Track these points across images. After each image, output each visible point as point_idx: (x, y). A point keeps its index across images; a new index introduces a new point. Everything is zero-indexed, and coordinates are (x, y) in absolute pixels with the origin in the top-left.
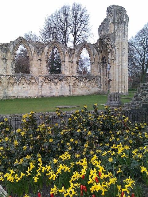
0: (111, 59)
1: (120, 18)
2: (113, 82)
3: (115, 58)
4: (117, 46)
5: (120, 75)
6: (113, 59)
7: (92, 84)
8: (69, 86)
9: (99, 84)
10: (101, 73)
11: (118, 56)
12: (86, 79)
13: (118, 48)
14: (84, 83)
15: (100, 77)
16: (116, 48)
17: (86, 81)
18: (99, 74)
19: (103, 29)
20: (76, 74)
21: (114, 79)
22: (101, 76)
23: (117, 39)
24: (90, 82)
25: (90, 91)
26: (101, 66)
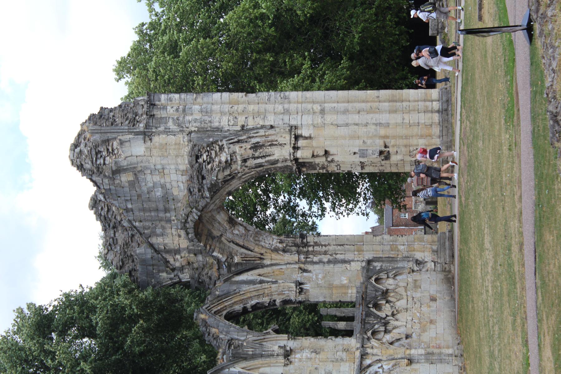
0: (296, 148)
1: (130, 116)
2: (394, 137)
3: (292, 128)
4: (241, 120)
5: (363, 105)
6: (297, 137)
7: (401, 290)
8: (411, 361)
9: (400, 265)
10: (349, 256)
11: (286, 118)
12: (377, 306)
13: (250, 119)
14: (399, 316)
15: (369, 262)
16: (251, 124)
17: (386, 310)
18: (357, 266)
19: (153, 240)
20: (352, 342)
21: (382, 132)
22: (369, 256)
23: (216, 124)
24: (392, 294)
25: (438, 295)
26: (316, 259)
